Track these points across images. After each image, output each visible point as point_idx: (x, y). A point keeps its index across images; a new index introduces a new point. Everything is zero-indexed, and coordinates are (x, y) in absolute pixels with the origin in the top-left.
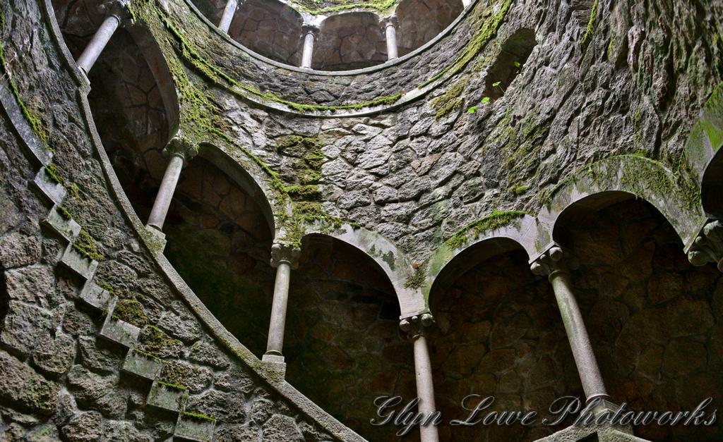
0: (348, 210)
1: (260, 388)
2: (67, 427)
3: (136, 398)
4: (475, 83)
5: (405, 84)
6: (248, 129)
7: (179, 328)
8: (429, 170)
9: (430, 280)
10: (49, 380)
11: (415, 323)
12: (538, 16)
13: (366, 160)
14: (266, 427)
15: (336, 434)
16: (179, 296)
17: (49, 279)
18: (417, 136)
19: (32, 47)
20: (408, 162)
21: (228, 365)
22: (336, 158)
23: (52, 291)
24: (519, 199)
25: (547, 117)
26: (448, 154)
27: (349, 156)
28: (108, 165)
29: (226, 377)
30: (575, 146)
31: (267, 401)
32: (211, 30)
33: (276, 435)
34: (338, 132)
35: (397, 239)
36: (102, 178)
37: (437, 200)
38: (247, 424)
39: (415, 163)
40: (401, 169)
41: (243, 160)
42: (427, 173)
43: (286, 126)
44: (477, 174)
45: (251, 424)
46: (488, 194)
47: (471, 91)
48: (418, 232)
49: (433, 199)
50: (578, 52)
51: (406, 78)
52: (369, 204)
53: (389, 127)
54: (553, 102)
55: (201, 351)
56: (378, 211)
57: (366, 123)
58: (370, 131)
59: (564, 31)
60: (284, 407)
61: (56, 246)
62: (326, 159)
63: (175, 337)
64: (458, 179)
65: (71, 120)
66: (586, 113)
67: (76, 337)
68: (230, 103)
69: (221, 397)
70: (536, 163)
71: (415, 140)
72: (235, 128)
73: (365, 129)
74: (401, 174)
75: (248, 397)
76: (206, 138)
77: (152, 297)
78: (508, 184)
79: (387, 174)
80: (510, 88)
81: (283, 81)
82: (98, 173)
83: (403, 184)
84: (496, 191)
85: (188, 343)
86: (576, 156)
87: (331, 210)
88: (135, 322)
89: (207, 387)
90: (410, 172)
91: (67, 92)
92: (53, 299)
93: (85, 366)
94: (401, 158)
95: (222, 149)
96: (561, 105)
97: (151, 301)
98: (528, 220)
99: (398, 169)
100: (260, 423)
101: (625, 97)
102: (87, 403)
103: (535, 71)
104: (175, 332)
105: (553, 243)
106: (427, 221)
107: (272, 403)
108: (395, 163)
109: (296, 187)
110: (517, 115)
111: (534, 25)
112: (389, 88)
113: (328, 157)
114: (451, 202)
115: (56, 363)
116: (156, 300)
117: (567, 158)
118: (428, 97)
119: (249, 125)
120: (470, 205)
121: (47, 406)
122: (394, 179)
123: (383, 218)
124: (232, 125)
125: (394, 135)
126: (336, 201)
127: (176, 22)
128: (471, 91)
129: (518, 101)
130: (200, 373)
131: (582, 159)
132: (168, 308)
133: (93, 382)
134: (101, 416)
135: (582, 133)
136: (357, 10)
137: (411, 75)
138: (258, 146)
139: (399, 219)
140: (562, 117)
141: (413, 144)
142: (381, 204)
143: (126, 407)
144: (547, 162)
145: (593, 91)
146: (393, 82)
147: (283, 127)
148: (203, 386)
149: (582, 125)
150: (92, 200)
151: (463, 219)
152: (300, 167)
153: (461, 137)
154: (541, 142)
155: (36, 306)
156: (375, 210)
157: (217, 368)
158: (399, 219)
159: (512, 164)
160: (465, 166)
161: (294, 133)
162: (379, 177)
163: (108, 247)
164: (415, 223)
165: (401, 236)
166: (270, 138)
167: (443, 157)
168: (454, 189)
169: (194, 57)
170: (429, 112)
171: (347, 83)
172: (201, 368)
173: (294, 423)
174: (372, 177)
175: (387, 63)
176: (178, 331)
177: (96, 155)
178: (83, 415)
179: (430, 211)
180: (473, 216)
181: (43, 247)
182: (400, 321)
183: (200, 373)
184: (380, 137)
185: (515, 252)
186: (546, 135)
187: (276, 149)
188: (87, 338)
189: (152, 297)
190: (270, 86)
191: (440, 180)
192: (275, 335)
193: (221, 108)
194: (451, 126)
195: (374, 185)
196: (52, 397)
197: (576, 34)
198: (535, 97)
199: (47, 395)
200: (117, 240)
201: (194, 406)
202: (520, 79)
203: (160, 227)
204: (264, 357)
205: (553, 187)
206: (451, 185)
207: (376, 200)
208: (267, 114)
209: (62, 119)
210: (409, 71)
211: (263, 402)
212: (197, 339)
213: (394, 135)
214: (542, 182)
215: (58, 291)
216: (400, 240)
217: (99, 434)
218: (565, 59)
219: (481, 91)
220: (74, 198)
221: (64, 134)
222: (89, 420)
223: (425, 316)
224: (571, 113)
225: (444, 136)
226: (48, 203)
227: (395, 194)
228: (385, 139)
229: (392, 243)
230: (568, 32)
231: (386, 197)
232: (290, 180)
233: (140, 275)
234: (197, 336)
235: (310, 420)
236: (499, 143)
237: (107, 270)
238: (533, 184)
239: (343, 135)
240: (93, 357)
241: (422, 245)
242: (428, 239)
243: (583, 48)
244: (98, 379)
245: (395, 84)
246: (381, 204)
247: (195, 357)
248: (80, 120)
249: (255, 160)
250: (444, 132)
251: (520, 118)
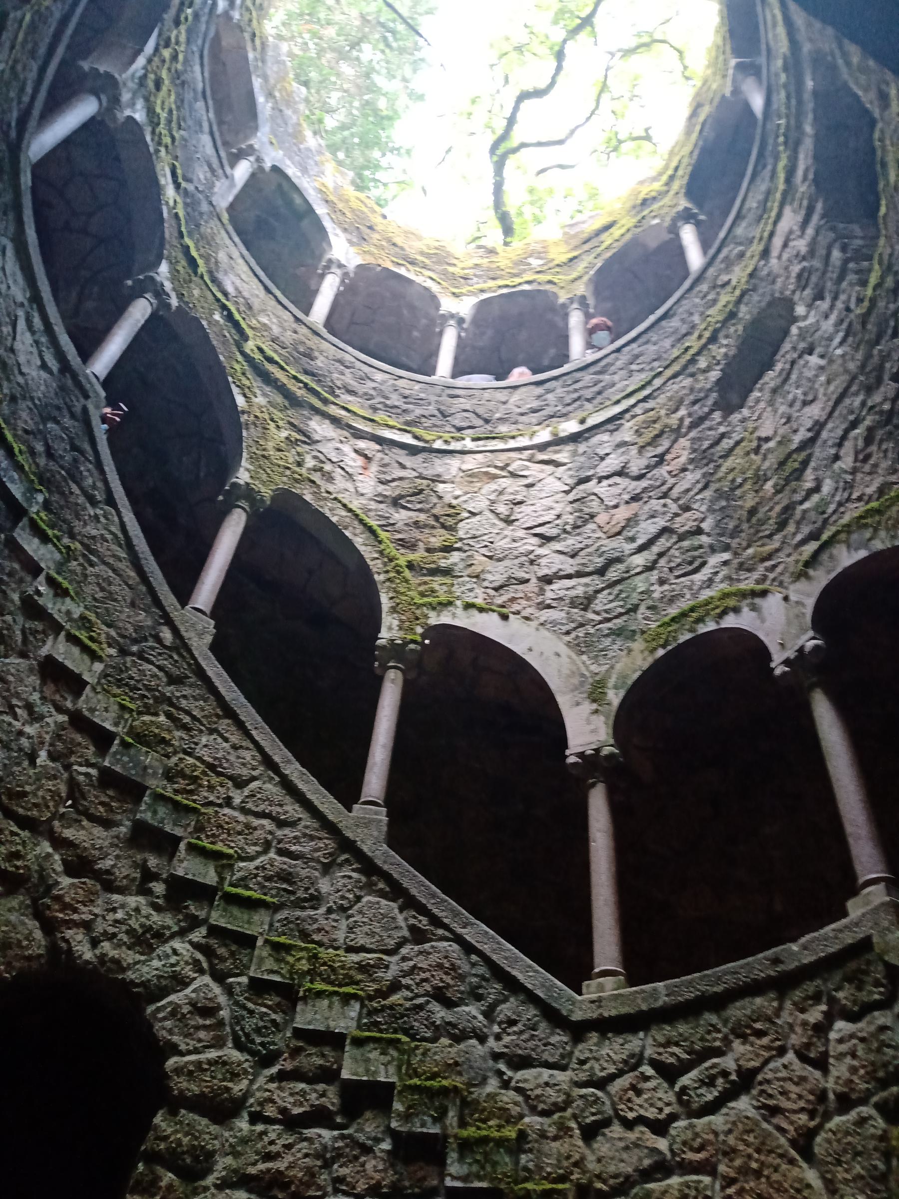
0: (496, 589)
1: (346, 856)
2: (47, 901)
3: (153, 862)
4: (701, 390)
5: (593, 398)
6: (348, 469)
7: (227, 760)
8: (624, 528)
9: (615, 698)
10: (23, 829)
11: (592, 762)
12: (799, 276)
13: (526, 515)
14: (352, 916)
15: (460, 931)
16: (229, 713)
17: (34, 680)
18: (607, 477)
19: (14, 338)
20: (592, 516)
21: (300, 819)
22: (480, 513)
23: (36, 697)
24: (761, 568)
25: (810, 435)
26: (654, 502)
27: (502, 509)
28: (129, 517)
29: (295, 838)
30: (849, 478)
31: (354, 875)
32: (297, 320)
33: (366, 929)
34: (486, 473)
35: (568, 633)
36: (120, 535)
37: (633, 572)
38: (322, 910)
39: (602, 519)
40: (579, 527)
41: (337, 516)
42: (619, 533)
43: (408, 464)
44: (699, 531)
45: (330, 911)
46: (714, 560)
47: (694, 403)
48: (600, 622)
49: (627, 572)
50: (857, 327)
51: (596, 389)
52: (527, 581)
53: (564, 464)
54: (815, 411)
55: (259, 796)
56: (542, 592)
57: (529, 460)
58: (535, 471)
59: (835, 298)
60: (381, 885)
61: (44, 632)
62: (466, 515)
63: (219, 774)
64: (667, 541)
65: (74, 448)
66: (868, 422)
67: (68, 767)
68: (319, 428)
69: (285, 867)
70: (789, 509)
71: (605, 483)
72: (328, 467)
73: (527, 468)
74: (579, 534)
75: (326, 869)
76: (282, 482)
77: (188, 713)
78: (744, 544)
79: (559, 535)
80: (756, 394)
81: (405, 397)
82: (113, 529)
83: (582, 549)
84: (726, 556)
85: (240, 783)
86: (850, 494)
87: (471, 590)
88: (159, 749)
89: (266, 851)
90: (594, 531)
91: (69, 408)
92: (37, 709)
93: (79, 812)
94: (581, 511)
95: (308, 497)
96: (830, 415)
97: (187, 719)
98: (773, 603)
99: (576, 527)
100: (343, 909)
102: (80, 865)
103: (793, 363)
104: (221, 766)
105: (811, 633)
106: (616, 606)
107: (364, 879)
108: (570, 519)
109: (417, 556)
110: (763, 435)
111: (794, 292)
112: (569, 405)
113: (470, 512)
114: (654, 576)
115: (36, 805)
116: (194, 718)
117: (837, 498)
118: (627, 416)
119: (351, 463)
120: (682, 579)
121: (18, 868)
122: (571, 542)
123: (548, 602)
124: (323, 462)
125: (571, 477)
126: (477, 577)
127: (242, 308)
128: (694, 403)
129: (764, 417)
130: (255, 829)
131: (859, 499)
132: (211, 731)
133: (86, 835)
134: (99, 887)
135: (861, 457)
136: (526, 287)
137: (602, 384)
138: (362, 495)
139: (573, 604)
141: (602, 489)
142: (547, 580)
143: (138, 875)
144: (807, 505)
145: (878, 387)
146: (575, 395)
147: (403, 466)
148: (258, 849)
149: (860, 443)
150: (102, 567)
151: (672, 600)
152: (426, 526)
153: (675, 476)
154: (798, 474)
155: (8, 718)
156: (536, 590)
157: (281, 824)
158: (573, 604)
159: (752, 512)
160: (678, 519)
161: (421, 477)
162: (546, 539)
163: (124, 637)
164: (598, 608)
165: (575, 629)
166: (381, 482)
167: (646, 508)
168: (661, 555)
169: (270, 360)
170: (627, 439)
171: (504, 400)
172: (256, 822)
173: (396, 911)
174: (535, 541)
175: (566, 368)
176: (225, 765)
177: (111, 501)
178: (73, 884)
179: (621, 591)
180: (688, 596)
181: (23, 631)
182: (567, 757)
183: (255, 829)
184: (551, 479)
185: (752, 648)
186: (805, 463)
187: (389, 500)
188: (83, 769)
189: (188, 713)
190: (386, 406)
191: (640, 542)
192: (375, 780)
193: (309, 437)
194: (661, 459)
195: (536, 553)
196: (27, 854)
197: (853, 300)
198: (791, 405)
199: (18, 851)
200: (138, 628)
201: (243, 879)
202: (770, 378)
203: (208, 612)
204: (356, 807)
205: (813, 546)
206: (656, 549)
207: (540, 574)
208: (378, 447)
209: (60, 448)
210: (601, 377)
211: (350, 877)
212: (254, 779)
213: (571, 477)
214: (799, 537)
215: (43, 698)
216: (573, 635)
217: (95, 915)
218: (837, 340)
219: (710, 402)
220: (75, 563)
221: (62, 467)
222: (81, 891)
223: (606, 751)
224: (844, 426)
225: (649, 475)
226: (34, 569)
227: (569, 566)
228: (558, 483)
229: (561, 639)
230: (843, 297)
231: (554, 570)
232: (411, 546)
233: (173, 680)
234: (255, 773)
235: (422, 910)
236: (733, 481)
237: (122, 671)
238: (783, 543)
239: (495, 477)
240: (95, 799)
241: (607, 642)
242: (617, 633)
243: (864, 319)
244: (98, 831)
245: (579, 398)
246: (547, 580)
247: (250, 805)
248: (87, 447)
249: (357, 516)
250: (649, 468)
251: (767, 439)
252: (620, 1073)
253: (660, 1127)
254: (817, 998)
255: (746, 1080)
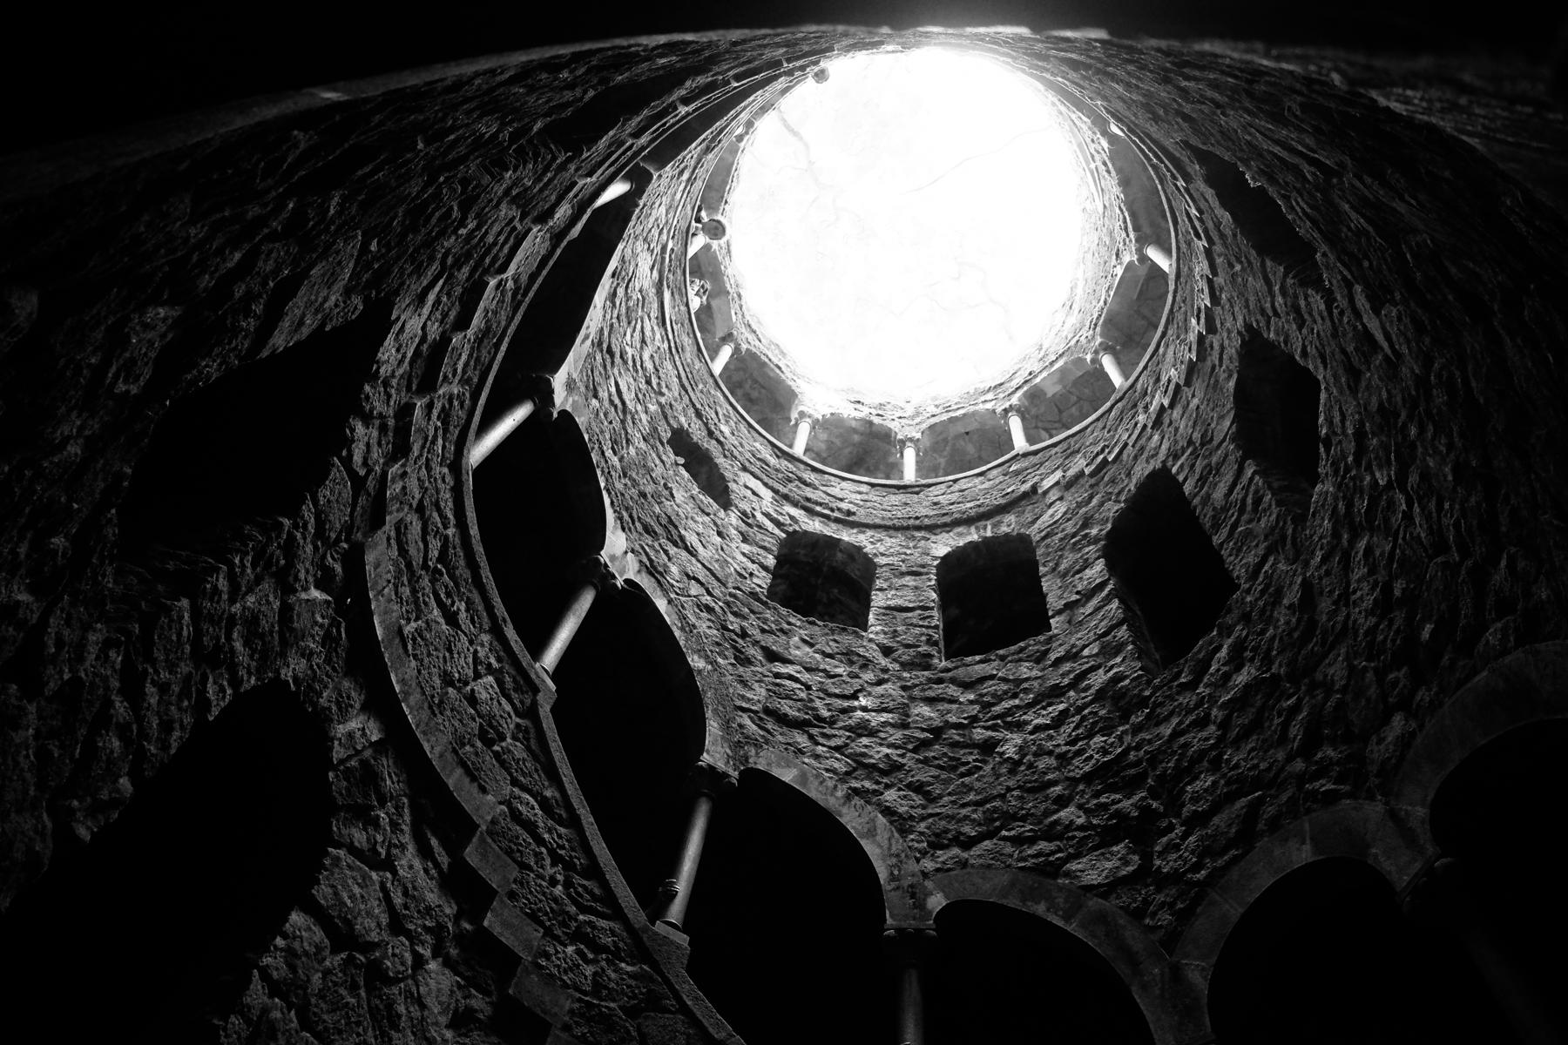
12: (744, 513)
101: (751, 663)
140: (696, 569)
206: (617, 401)
243: (753, 595)
252: (441, 516)
253: (425, 566)
254: (499, 660)
255: (452, 619)
